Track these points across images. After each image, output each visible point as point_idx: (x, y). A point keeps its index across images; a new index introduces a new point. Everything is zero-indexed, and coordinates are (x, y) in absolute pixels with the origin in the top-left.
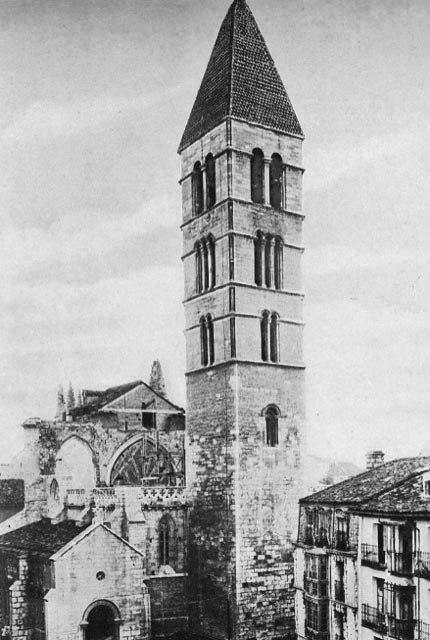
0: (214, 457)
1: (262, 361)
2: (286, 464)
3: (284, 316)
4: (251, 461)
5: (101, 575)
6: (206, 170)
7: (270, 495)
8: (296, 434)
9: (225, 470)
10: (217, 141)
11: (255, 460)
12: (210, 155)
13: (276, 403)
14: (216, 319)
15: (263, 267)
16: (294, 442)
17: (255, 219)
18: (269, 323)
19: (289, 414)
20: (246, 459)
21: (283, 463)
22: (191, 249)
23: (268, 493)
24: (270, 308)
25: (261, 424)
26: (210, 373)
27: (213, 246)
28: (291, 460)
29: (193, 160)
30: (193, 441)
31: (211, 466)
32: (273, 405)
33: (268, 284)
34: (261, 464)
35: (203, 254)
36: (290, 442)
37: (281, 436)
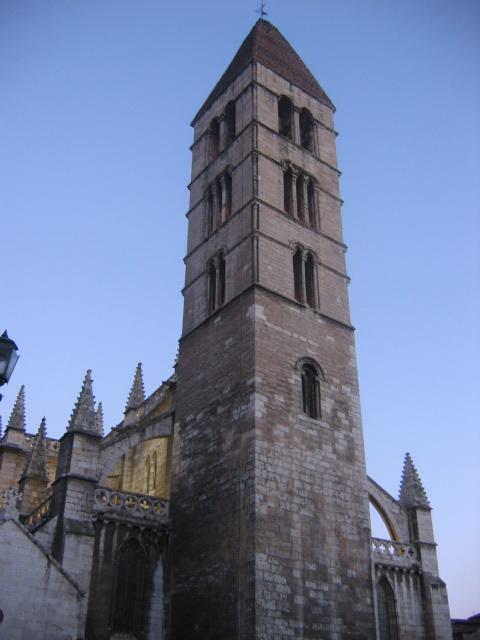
2: (335, 451)
3: (322, 258)
4: (280, 430)
7: (312, 492)
8: (346, 411)
9: (236, 443)
11: (287, 430)
13: (317, 359)
18: (304, 264)
20: (273, 424)
21: (330, 449)
23: (308, 487)
24: (307, 244)
25: (295, 379)
26: (219, 318)
28: (342, 446)
30: (184, 426)
31: (212, 447)
32: (313, 360)
33: (300, 214)
35: (215, 193)
36: (339, 420)
37: (326, 405)
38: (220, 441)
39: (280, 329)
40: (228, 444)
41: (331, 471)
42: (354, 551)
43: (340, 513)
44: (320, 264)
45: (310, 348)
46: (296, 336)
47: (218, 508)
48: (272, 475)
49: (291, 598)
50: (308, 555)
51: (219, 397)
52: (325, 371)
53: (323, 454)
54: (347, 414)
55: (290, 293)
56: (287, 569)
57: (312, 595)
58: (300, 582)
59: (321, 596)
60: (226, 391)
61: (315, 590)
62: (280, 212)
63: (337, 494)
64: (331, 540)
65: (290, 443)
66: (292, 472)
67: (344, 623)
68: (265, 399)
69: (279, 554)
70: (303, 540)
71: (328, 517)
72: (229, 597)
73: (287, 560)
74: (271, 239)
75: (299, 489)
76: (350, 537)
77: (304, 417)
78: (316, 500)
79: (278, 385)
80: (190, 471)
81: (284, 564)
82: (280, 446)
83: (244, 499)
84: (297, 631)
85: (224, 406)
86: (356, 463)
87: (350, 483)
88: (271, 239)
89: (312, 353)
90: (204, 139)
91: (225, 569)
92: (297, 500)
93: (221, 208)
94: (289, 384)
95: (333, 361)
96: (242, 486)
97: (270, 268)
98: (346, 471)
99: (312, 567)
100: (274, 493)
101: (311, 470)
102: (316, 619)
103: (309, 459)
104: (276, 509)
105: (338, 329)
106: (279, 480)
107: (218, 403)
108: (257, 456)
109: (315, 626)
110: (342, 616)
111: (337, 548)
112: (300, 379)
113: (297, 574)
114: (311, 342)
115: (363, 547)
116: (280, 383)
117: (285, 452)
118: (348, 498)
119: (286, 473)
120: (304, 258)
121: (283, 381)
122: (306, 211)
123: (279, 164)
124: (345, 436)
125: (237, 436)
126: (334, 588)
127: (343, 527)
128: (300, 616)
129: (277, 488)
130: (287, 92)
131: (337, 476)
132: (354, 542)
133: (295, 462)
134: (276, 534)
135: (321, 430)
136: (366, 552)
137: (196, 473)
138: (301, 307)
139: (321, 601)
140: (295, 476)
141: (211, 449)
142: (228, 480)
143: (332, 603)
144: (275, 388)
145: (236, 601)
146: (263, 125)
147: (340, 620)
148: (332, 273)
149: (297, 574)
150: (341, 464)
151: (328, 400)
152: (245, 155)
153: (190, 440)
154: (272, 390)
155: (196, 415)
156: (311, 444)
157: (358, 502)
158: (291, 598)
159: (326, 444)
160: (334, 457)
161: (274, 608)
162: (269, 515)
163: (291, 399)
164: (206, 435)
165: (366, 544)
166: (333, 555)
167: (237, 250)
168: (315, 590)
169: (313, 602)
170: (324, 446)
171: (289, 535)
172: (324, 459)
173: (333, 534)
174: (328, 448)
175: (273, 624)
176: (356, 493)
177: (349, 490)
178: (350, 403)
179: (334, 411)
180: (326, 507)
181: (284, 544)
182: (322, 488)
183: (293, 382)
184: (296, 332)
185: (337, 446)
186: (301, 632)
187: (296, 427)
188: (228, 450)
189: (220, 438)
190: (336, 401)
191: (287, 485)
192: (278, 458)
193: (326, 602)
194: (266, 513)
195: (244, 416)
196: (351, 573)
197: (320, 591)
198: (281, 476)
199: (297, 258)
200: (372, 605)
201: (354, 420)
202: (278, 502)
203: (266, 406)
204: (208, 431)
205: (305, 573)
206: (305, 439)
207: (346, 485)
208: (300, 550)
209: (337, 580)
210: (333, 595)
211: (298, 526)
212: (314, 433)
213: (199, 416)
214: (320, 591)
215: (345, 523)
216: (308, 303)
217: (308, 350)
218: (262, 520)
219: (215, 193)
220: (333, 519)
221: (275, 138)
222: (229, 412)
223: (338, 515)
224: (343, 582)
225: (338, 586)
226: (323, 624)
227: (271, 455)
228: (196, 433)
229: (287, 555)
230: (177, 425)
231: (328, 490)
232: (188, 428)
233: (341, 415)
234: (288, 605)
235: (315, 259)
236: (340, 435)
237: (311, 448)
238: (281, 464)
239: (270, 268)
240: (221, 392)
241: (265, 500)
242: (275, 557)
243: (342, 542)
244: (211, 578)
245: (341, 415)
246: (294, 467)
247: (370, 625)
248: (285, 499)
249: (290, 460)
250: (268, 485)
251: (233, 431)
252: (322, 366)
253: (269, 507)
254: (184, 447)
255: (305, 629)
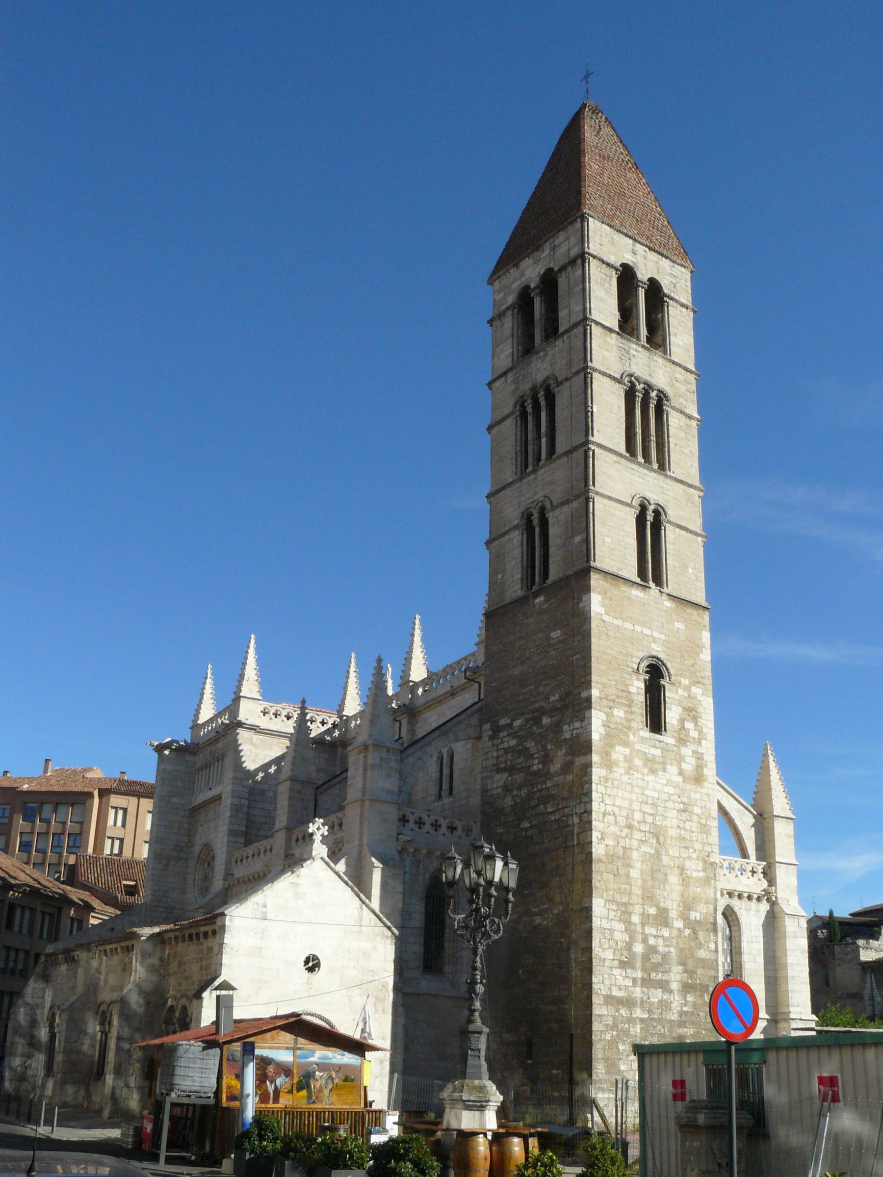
0: (544, 747)
1: (638, 580)
2: (681, 773)
4: (619, 753)
5: (312, 964)
6: (541, 293)
8: (695, 719)
9: (567, 767)
10: (563, 249)
11: (627, 751)
12: (550, 270)
14: (554, 508)
15: (639, 430)
16: (694, 734)
17: (625, 355)
19: (685, 682)
20: (612, 746)
22: (509, 409)
23: (649, 819)
24: (654, 498)
25: (638, 686)
26: (542, 599)
27: (551, 399)
29: (517, 286)
31: (536, 766)
33: (646, 455)
34: (638, 762)
35: (529, 409)
36: (687, 731)
37: (672, 715)
38: (546, 760)
39: (618, 622)
40: (556, 767)
41: (676, 797)
42: (699, 890)
43: (684, 847)
44: (670, 522)
45: (655, 642)
46: (638, 628)
47: (546, 841)
48: (609, 808)
49: (629, 946)
50: (649, 897)
51: (543, 704)
52: (672, 671)
53: (668, 776)
54: (696, 724)
55: (631, 572)
56: (625, 916)
57: (652, 941)
58: (639, 928)
59: (660, 941)
60: (553, 698)
61: (655, 937)
62: (621, 455)
63: (682, 826)
64: (674, 879)
65: (630, 768)
66: (631, 802)
67: (685, 971)
68: (604, 718)
69: (618, 898)
70: (645, 881)
71: (671, 853)
72: (561, 942)
73: (625, 904)
74: (609, 498)
75: (639, 822)
76: (695, 874)
77: (646, 733)
78: (657, 834)
79: (618, 697)
80: (507, 789)
81: (623, 909)
82: (619, 772)
83: (578, 834)
84: (634, 980)
85: (551, 717)
86: (706, 784)
87: (697, 810)
88: (609, 498)
89: (657, 650)
90: (509, 313)
91: (556, 911)
92: (637, 835)
93: (539, 438)
94: (630, 693)
95: (682, 656)
96: (576, 820)
97: (608, 540)
98: (693, 795)
99: (652, 911)
100: (613, 829)
101: (652, 797)
102: (655, 967)
103: (650, 787)
104: (614, 847)
105: (689, 610)
106: (617, 813)
107: (543, 712)
108: (594, 786)
109: (653, 975)
110: (683, 963)
111: (680, 888)
112: (642, 686)
113: (636, 919)
114: (656, 634)
115: (709, 884)
116: (620, 693)
117: (625, 778)
118: (693, 829)
119: (626, 804)
120: (650, 517)
121: (624, 691)
122: (653, 445)
123: (619, 381)
124: (694, 752)
125: (569, 758)
126: (675, 933)
127: (688, 864)
128: (639, 964)
129: (616, 823)
130: (628, 259)
131: (682, 802)
132: (699, 879)
133: (636, 790)
134: (615, 875)
135: (665, 749)
136: (712, 891)
137: (515, 792)
138: (646, 587)
139: (661, 949)
140: (636, 806)
141: (535, 768)
142: (558, 810)
143: (672, 950)
144: (614, 701)
145: (568, 949)
146: (597, 323)
147: (680, 968)
148: (683, 532)
149: (636, 919)
150: (688, 787)
151: (674, 708)
152: (574, 370)
153: (506, 751)
154: (611, 704)
155: (512, 720)
156: (654, 766)
157: (705, 832)
158: (629, 946)
159: (671, 764)
160: (680, 779)
161: (612, 958)
162: (606, 854)
163: (632, 713)
164: (528, 749)
165: (713, 882)
166: (676, 896)
167: (566, 509)
168: (655, 937)
169: (653, 949)
170: (669, 767)
171: (628, 876)
172: (669, 783)
173: (677, 871)
174: (673, 769)
175: (609, 975)
176: (703, 822)
177: (695, 818)
178: (700, 709)
179: (682, 721)
180: (669, 842)
181: (623, 886)
182: (665, 818)
183: (633, 689)
184: (642, 625)
185: (684, 766)
186: (639, 982)
187: (637, 747)
188: (557, 774)
189: (546, 755)
190: (684, 709)
191: (627, 818)
192: (618, 788)
193: (667, 949)
194: (603, 852)
195: (578, 736)
196: (695, 915)
197: (660, 937)
198: (620, 808)
199: (641, 520)
200: (716, 951)
201: (704, 731)
202: (617, 838)
203: (604, 726)
204: (530, 744)
205: (646, 919)
206: (649, 761)
207: (691, 813)
208: (640, 892)
209: (679, 924)
210: (674, 941)
211: (638, 865)
212: (657, 752)
213: (517, 723)
214: (660, 937)
215: (690, 858)
216: (654, 581)
217: (653, 646)
218: (600, 860)
219: (529, 409)
220: (677, 855)
221: (613, 339)
222: (557, 727)
223: (683, 849)
224: (685, 927)
225: (679, 930)
226: (662, 972)
227: (609, 784)
228: (513, 743)
229: (625, 899)
230: (487, 726)
231: (671, 821)
232: (502, 734)
233: (689, 725)
234: (625, 953)
235: (663, 517)
236: (687, 751)
237: (653, 771)
238: (620, 795)
239: (608, 540)
240: (547, 698)
241: (603, 838)
242: (613, 901)
243: (686, 881)
244: (538, 920)
245: (689, 725)
246: (634, 797)
247: (713, 973)
248: (624, 834)
249: (629, 788)
250: (606, 820)
251: (564, 751)
252: (669, 665)
253: (607, 845)
254: (498, 757)
255: (643, 979)
